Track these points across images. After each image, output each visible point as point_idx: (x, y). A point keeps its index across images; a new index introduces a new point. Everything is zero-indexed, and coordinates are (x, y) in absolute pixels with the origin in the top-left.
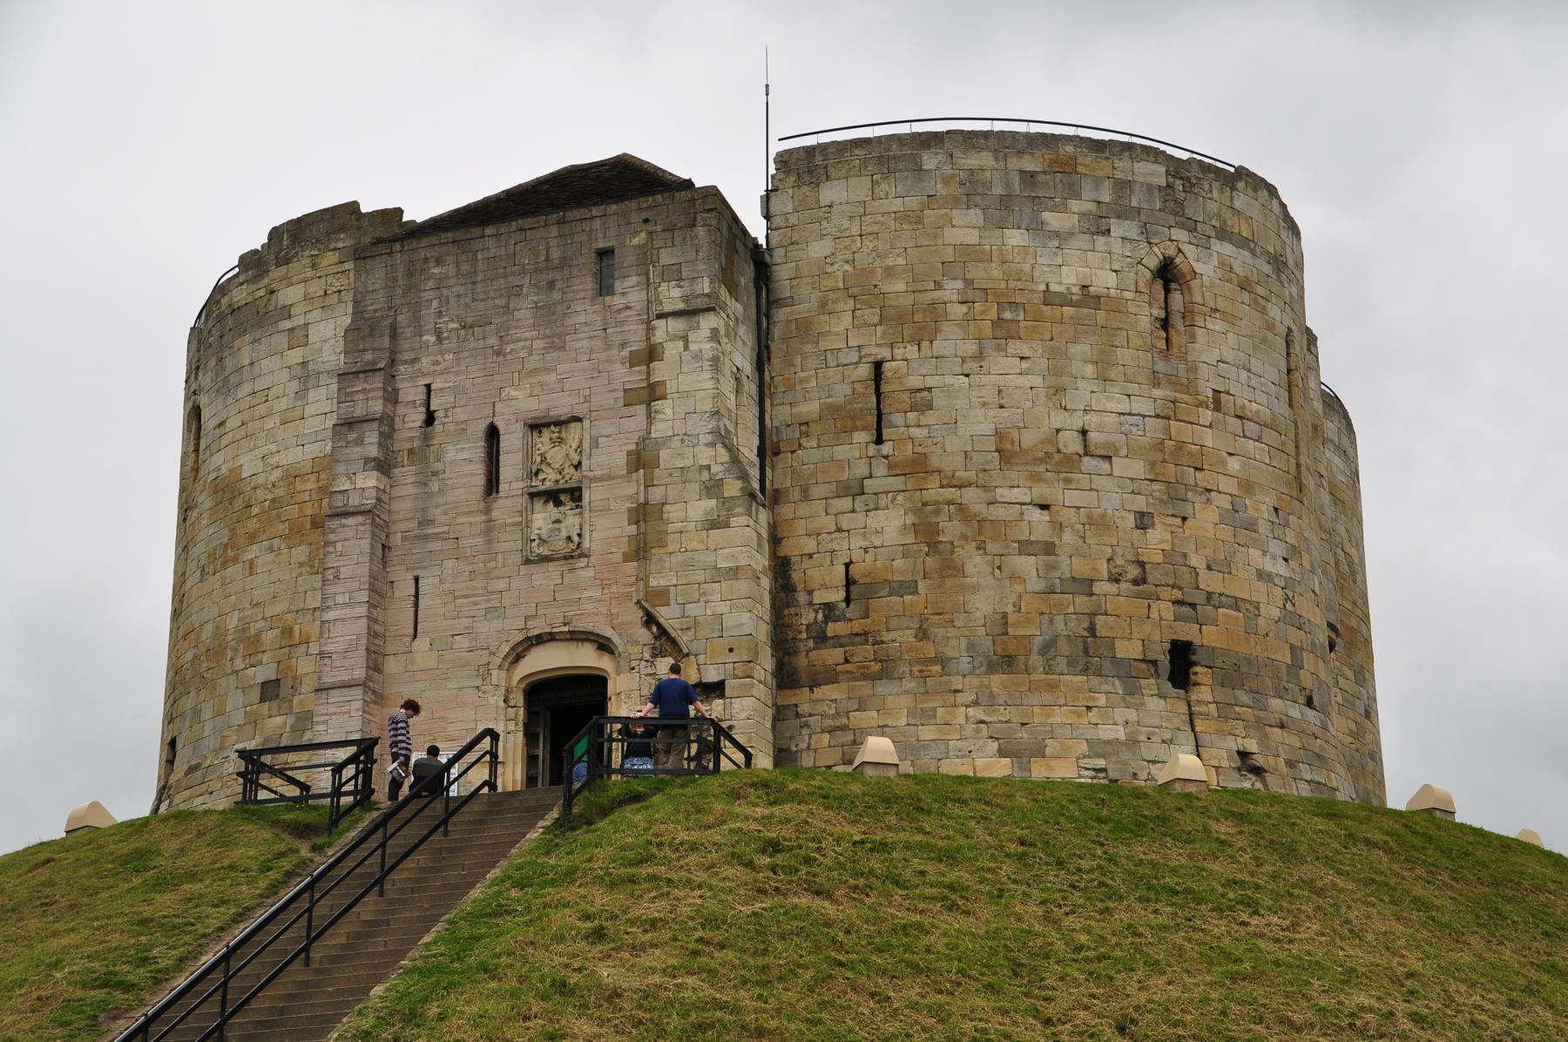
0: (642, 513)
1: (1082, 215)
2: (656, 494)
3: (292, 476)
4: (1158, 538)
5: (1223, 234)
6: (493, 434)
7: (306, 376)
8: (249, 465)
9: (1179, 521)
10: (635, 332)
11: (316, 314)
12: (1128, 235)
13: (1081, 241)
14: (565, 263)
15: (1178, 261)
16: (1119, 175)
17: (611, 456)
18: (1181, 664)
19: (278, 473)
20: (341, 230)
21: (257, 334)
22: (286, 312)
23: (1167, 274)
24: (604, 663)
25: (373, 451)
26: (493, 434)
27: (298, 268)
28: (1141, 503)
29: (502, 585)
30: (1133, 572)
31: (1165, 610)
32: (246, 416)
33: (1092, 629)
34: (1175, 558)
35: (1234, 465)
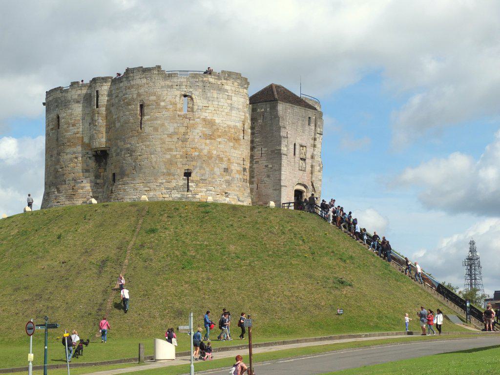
0: (312, 166)
2: (314, 164)
3: (229, 127)
6: (295, 145)
7: (232, 107)
8: (218, 120)
10: (313, 134)
11: (233, 95)
14: (304, 117)
17: (309, 155)
19: (226, 125)
20: (238, 79)
21: (219, 92)
22: (227, 91)
24: (305, 190)
25: (286, 144)
26: (295, 145)
27: (230, 82)
29: (295, 173)
32: (216, 109)
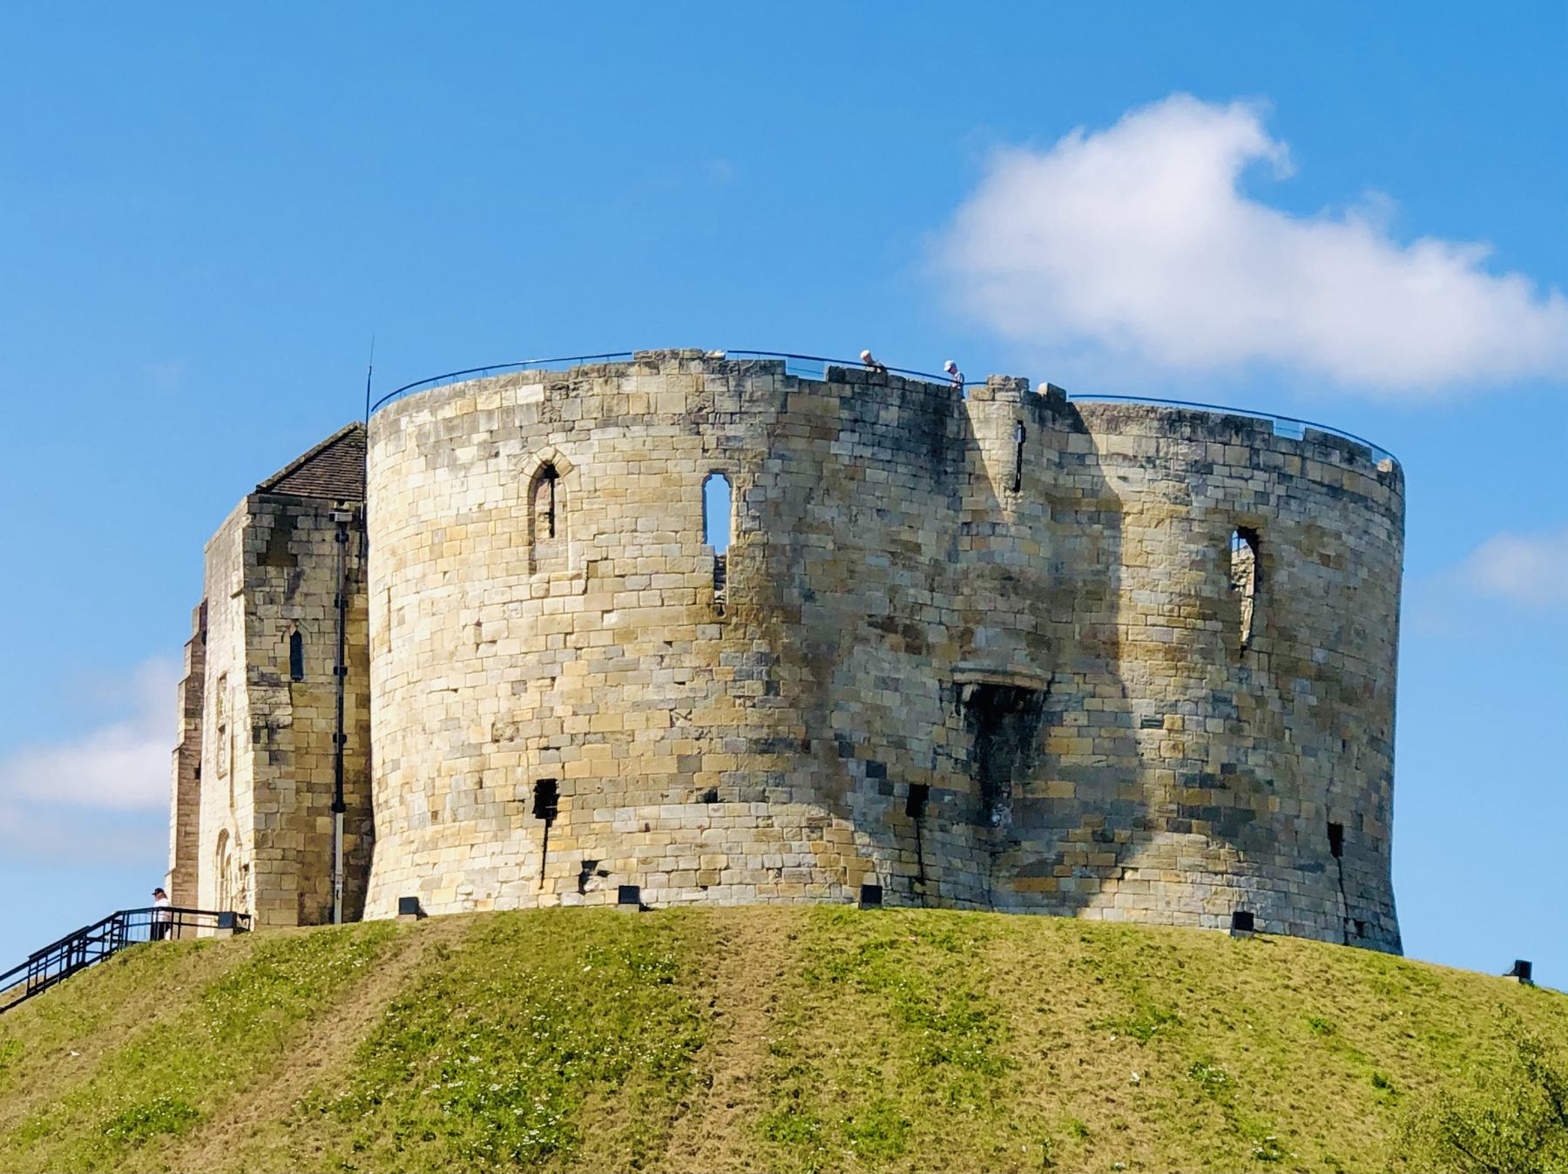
1: (479, 444)
4: (530, 699)
5: (606, 422)
9: (548, 681)
12: (513, 452)
13: (480, 467)
15: (555, 461)
16: (505, 403)
18: (546, 799)
23: (548, 473)
28: (516, 674)
30: (509, 732)
31: (533, 755)
33: (481, 784)
34: (539, 714)
35: (611, 619)
